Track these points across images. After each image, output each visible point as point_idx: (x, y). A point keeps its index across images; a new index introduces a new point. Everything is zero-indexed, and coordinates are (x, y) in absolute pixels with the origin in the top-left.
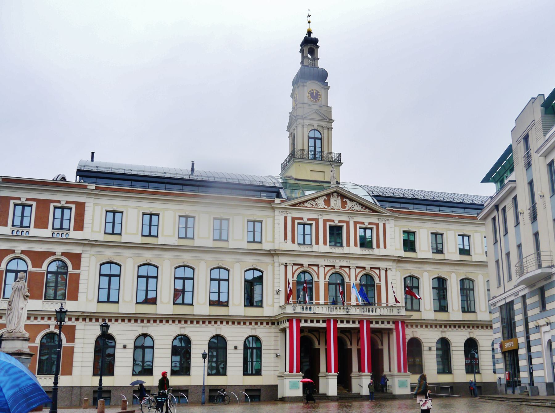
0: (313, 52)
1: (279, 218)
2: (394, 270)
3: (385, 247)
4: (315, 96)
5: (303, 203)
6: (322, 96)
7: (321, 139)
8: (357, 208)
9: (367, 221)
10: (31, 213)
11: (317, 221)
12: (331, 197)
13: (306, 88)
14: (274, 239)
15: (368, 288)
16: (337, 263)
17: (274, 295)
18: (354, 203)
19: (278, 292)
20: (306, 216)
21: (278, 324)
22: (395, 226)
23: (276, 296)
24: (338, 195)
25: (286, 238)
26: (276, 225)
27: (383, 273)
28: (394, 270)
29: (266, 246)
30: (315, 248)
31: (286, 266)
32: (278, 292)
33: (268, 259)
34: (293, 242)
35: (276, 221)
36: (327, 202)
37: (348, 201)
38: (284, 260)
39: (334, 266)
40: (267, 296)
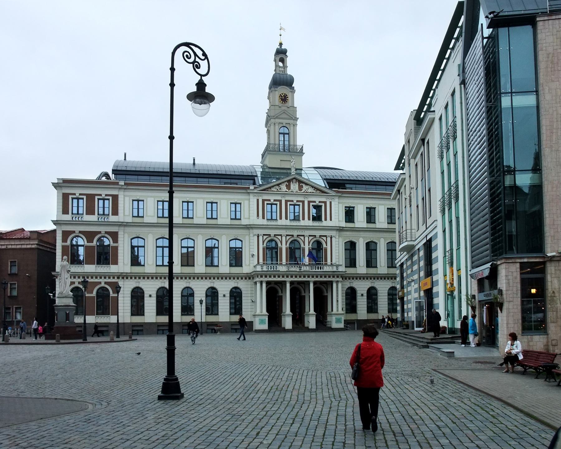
0: (282, 60)
1: (253, 200)
3: (331, 220)
4: (284, 99)
6: (290, 98)
7: (288, 134)
10: (83, 204)
11: (280, 201)
13: (277, 92)
14: (249, 216)
15: (318, 252)
23: (251, 259)
25: (258, 215)
27: (329, 239)
28: (337, 237)
29: (244, 222)
30: (280, 222)
31: (258, 236)
32: (253, 255)
34: (263, 218)
35: (251, 203)
38: (257, 232)
39: (293, 236)
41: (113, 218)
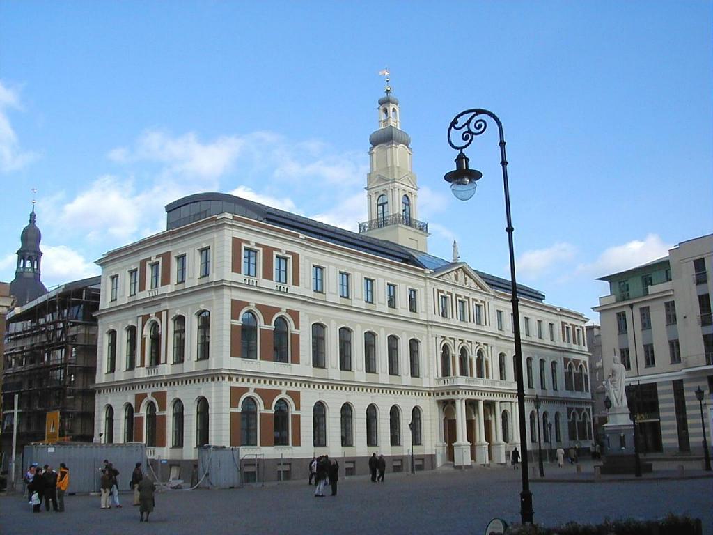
8: (473, 285)
9: (480, 298)
27: (489, 348)
33: (424, 329)
37: (468, 277)
41: (293, 289)
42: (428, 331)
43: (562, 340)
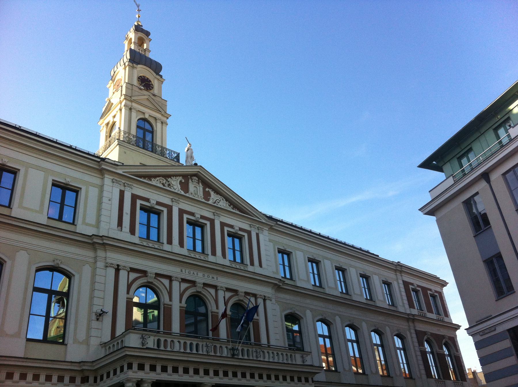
2: (273, 300)
5: (150, 177)
8: (223, 204)
12: (190, 181)
16: (200, 277)
17: (89, 321)
18: (220, 197)
19: (100, 315)
20: (155, 197)
21: (95, 381)
22: (270, 241)
23: (95, 324)
24: (198, 181)
25: (120, 223)
26: (105, 200)
27: (260, 301)
28: (273, 300)
31: (118, 270)
32: (100, 315)
33: (87, 254)
35: (105, 194)
36: (185, 187)
37: (212, 193)
40: (76, 323)
42: (96, 258)
43: (407, 306)
